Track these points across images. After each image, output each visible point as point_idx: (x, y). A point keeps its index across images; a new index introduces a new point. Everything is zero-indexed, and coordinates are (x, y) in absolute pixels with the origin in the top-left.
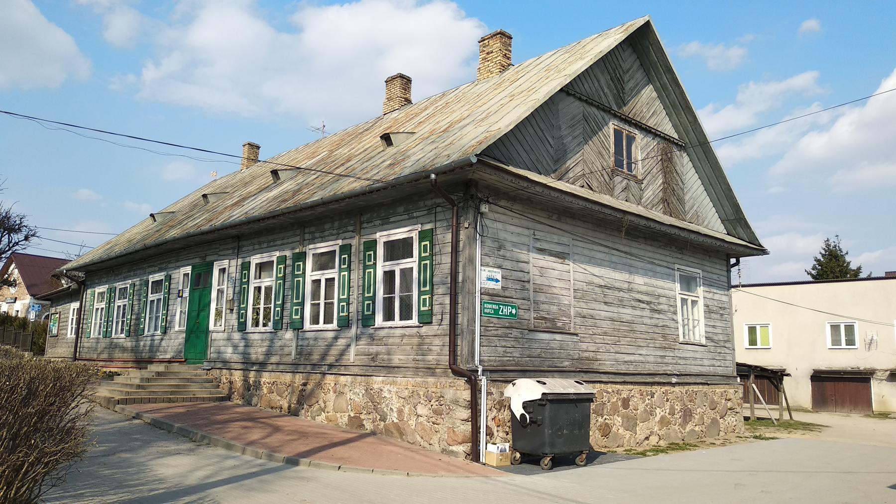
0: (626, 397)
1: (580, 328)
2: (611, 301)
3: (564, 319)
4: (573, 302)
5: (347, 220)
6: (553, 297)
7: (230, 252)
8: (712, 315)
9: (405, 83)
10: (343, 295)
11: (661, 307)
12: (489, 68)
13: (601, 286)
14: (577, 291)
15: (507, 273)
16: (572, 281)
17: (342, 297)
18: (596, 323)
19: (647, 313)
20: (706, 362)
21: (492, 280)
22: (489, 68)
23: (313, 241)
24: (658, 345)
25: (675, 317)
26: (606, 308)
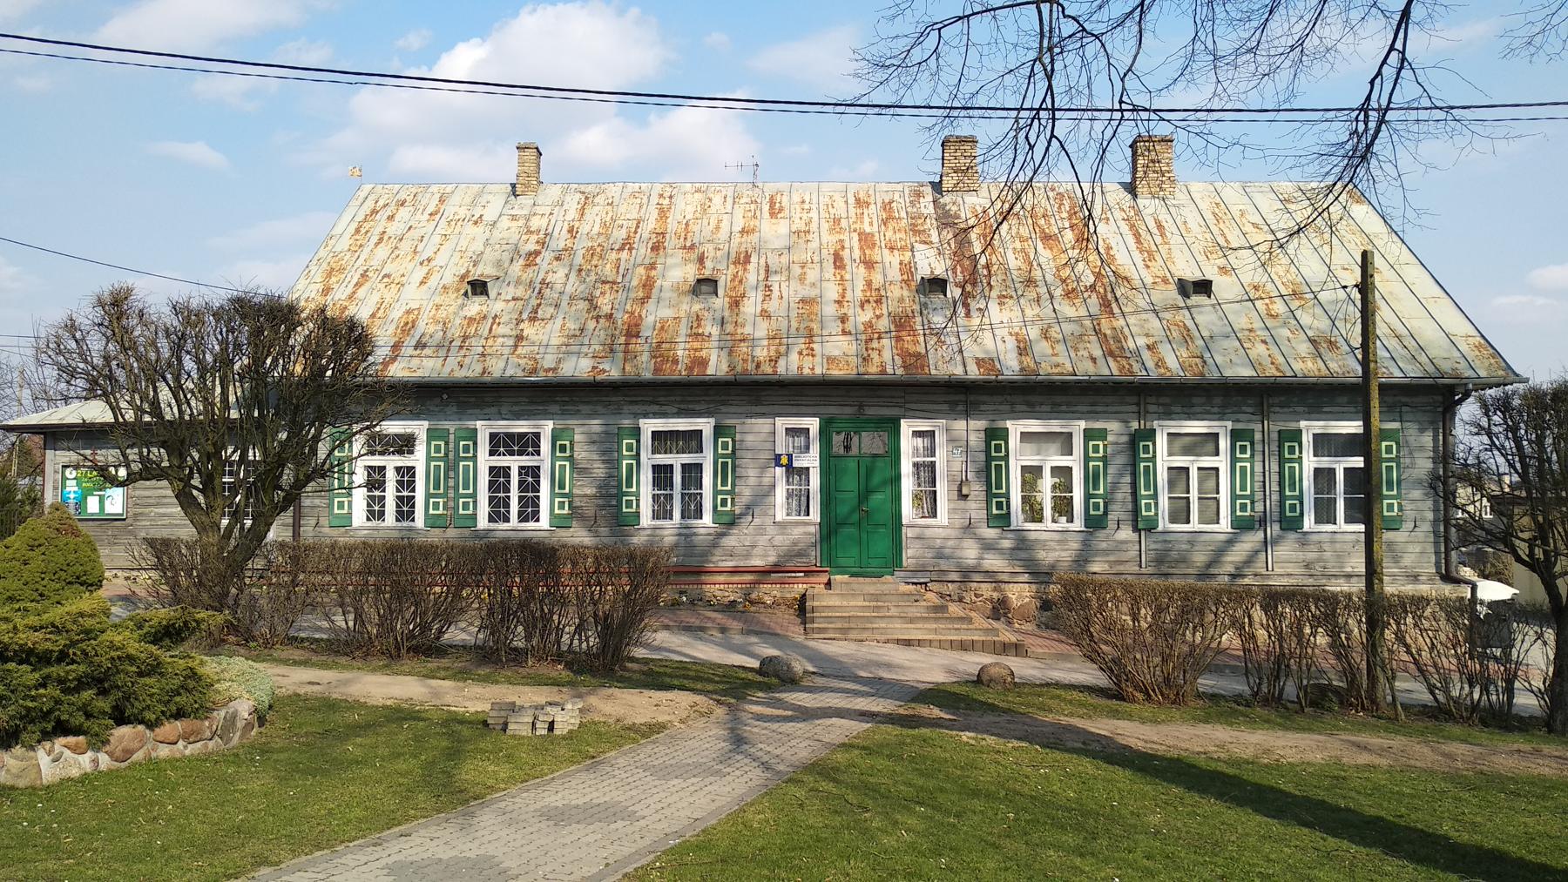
5: (1240, 398)
7: (945, 407)
23: (1168, 415)
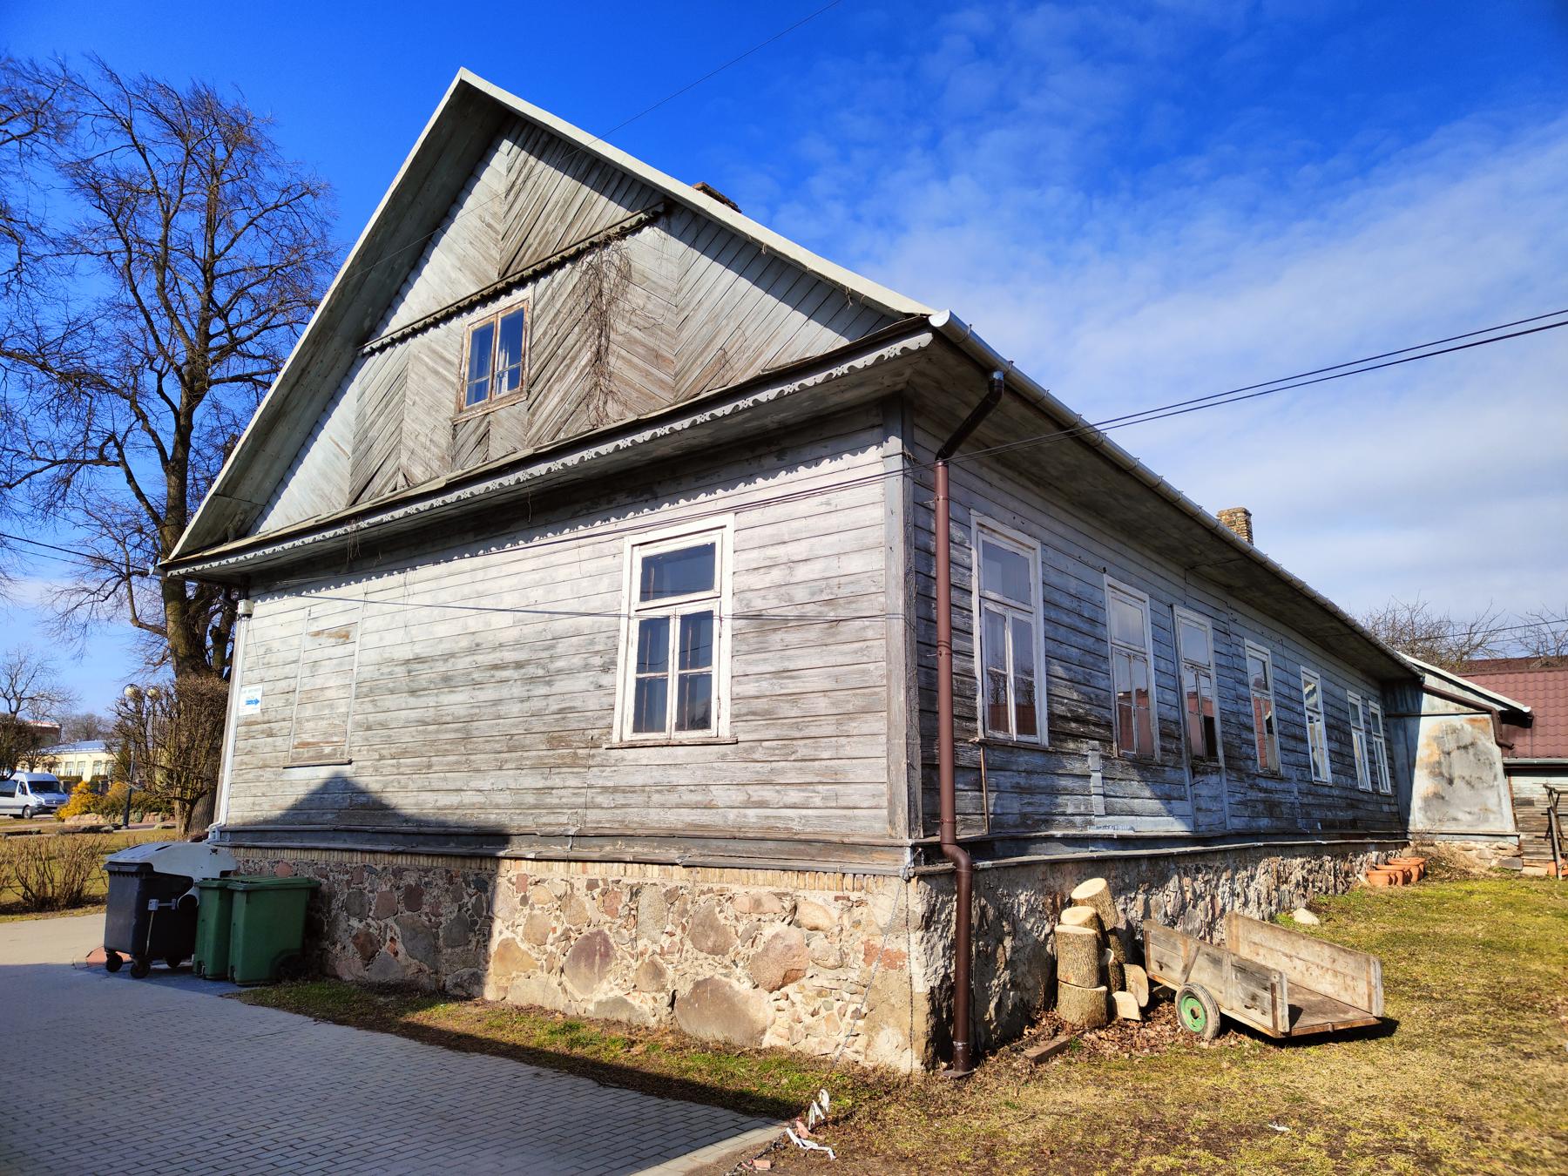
3: (335, 739)
11: (560, 664)
18: (389, 736)
19: (518, 690)
25: (605, 680)
26: (412, 701)
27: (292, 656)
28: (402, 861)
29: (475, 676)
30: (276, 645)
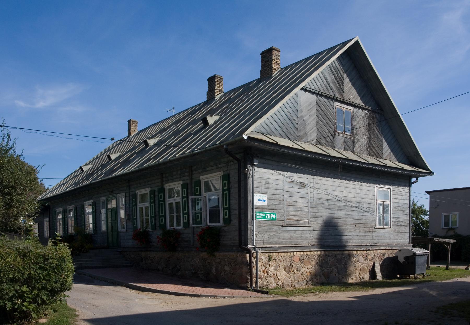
0: (340, 258)
1: (314, 223)
2: (334, 208)
4: (310, 210)
6: (297, 207)
8: (398, 211)
9: (219, 80)
10: (185, 210)
11: (364, 209)
12: (266, 71)
13: (328, 200)
14: (313, 203)
15: (270, 196)
16: (309, 198)
17: (185, 212)
19: (356, 213)
20: (392, 238)
21: (262, 200)
22: (266, 71)
24: (361, 230)
27: (281, 187)
28: (336, 253)
29: (347, 208)
30: (271, 181)
